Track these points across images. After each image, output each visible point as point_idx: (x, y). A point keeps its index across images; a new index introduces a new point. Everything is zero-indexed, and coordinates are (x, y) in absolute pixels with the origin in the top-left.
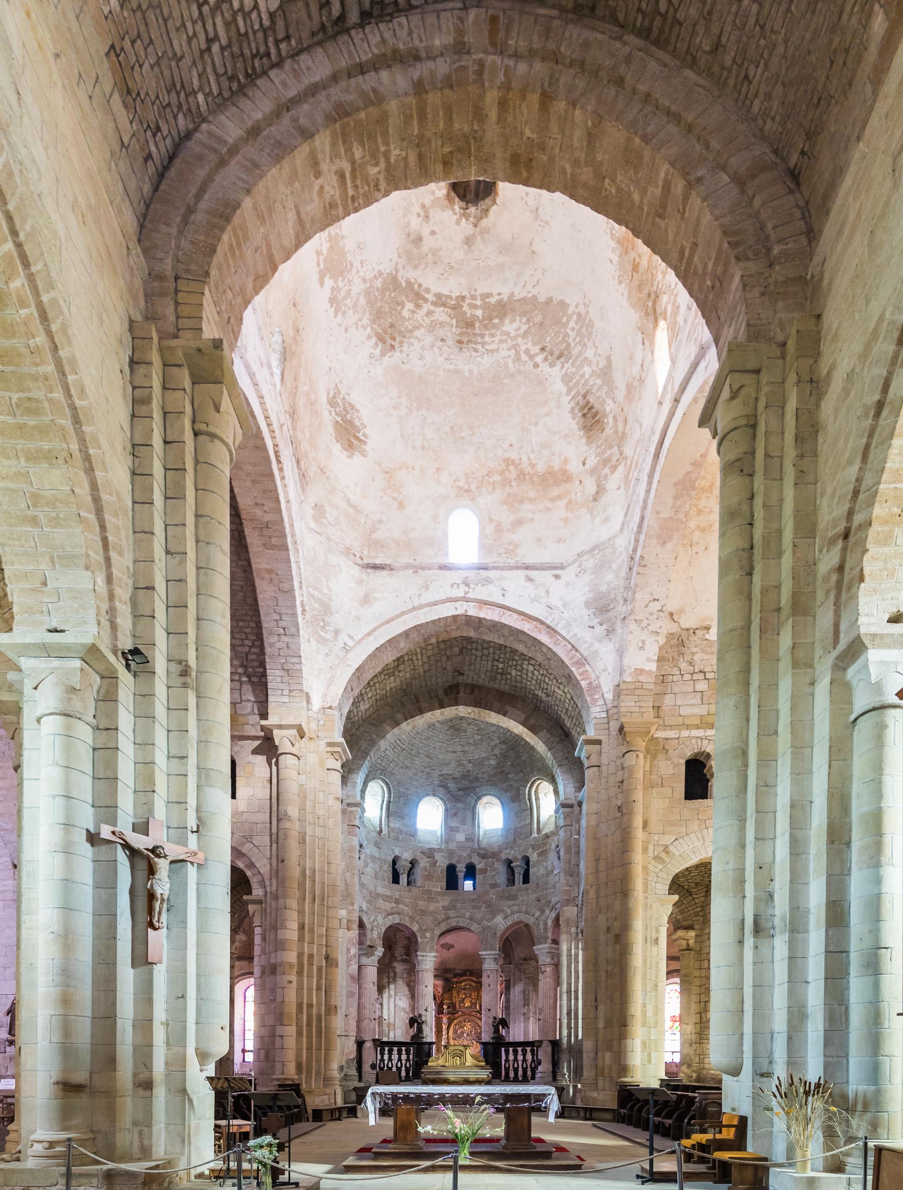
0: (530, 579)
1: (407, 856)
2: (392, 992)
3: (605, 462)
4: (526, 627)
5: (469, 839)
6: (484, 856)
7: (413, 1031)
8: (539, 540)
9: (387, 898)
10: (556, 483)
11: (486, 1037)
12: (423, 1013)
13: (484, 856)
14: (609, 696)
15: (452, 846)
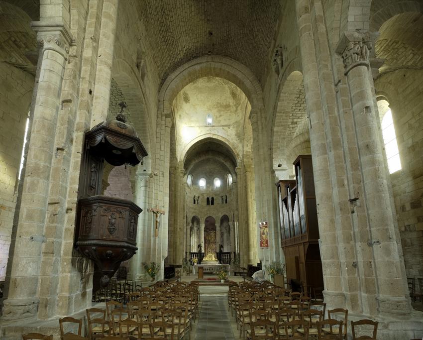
0: (223, 129)
1: (197, 195)
3: (237, 104)
5: (212, 190)
6: (216, 195)
7: (199, 249)
9: (193, 208)
10: (228, 107)
11: (218, 251)
13: (216, 195)
14: (241, 157)
15: (208, 192)
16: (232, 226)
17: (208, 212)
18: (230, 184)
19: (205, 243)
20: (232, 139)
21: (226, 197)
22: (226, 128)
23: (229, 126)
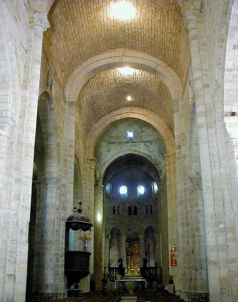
0: (145, 145)
1: (117, 205)
2: (113, 249)
4: (145, 156)
6: (139, 204)
7: (119, 264)
8: (147, 135)
9: (112, 219)
12: (123, 257)
16: (157, 239)
17: (130, 223)
18: (155, 183)
19: (127, 255)
20: (154, 156)
21: (151, 206)
22: (148, 144)
23: (151, 142)
